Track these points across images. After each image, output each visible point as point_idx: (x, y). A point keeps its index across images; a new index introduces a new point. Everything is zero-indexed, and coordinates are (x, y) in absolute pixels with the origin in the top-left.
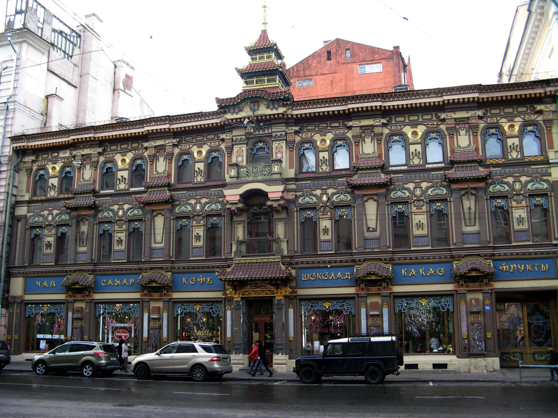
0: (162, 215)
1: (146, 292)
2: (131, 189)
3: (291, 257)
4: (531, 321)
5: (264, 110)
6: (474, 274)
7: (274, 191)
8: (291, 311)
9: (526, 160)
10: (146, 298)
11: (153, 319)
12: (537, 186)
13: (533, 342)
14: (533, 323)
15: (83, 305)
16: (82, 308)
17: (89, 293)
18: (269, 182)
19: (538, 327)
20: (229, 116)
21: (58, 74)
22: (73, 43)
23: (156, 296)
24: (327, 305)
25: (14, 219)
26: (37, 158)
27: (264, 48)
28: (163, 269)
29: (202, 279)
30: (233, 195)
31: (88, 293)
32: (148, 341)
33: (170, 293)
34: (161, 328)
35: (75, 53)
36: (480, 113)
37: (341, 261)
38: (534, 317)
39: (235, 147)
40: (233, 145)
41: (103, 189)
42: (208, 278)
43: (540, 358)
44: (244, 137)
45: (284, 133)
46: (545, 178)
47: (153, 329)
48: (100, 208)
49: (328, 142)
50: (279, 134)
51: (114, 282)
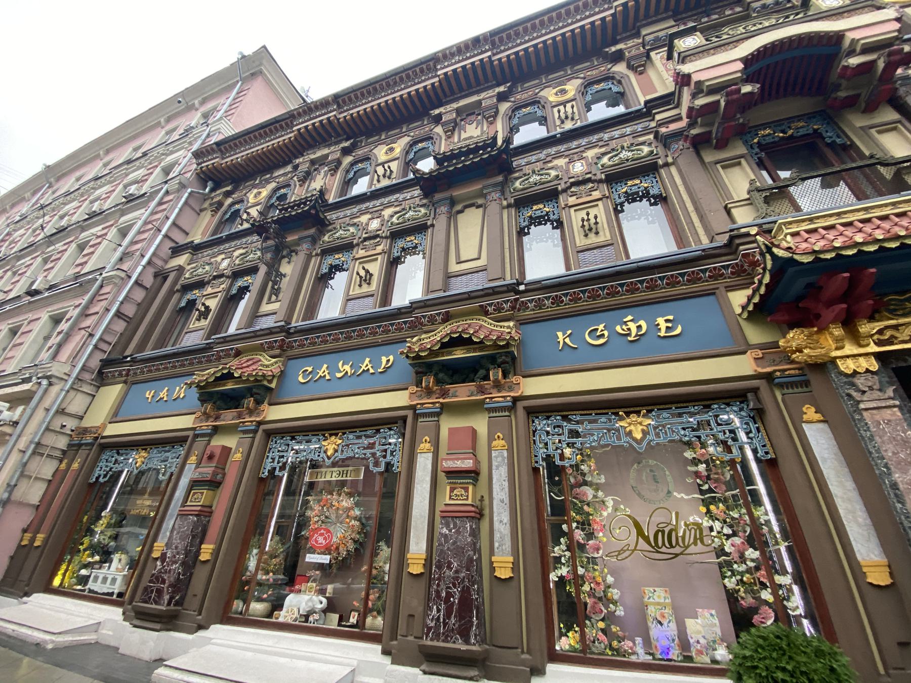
0: (478, 207)
1: (429, 381)
10: (430, 403)
11: (452, 474)
16: (226, 451)
17: (259, 402)
23: (463, 392)
25: (161, 276)
28: (486, 313)
29: (633, 326)
31: (251, 405)
32: (426, 577)
33: (514, 379)
34: (478, 514)
39: (652, 54)
42: (661, 321)
47: (450, 516)
48: (330, 227)
51: (333, 369)
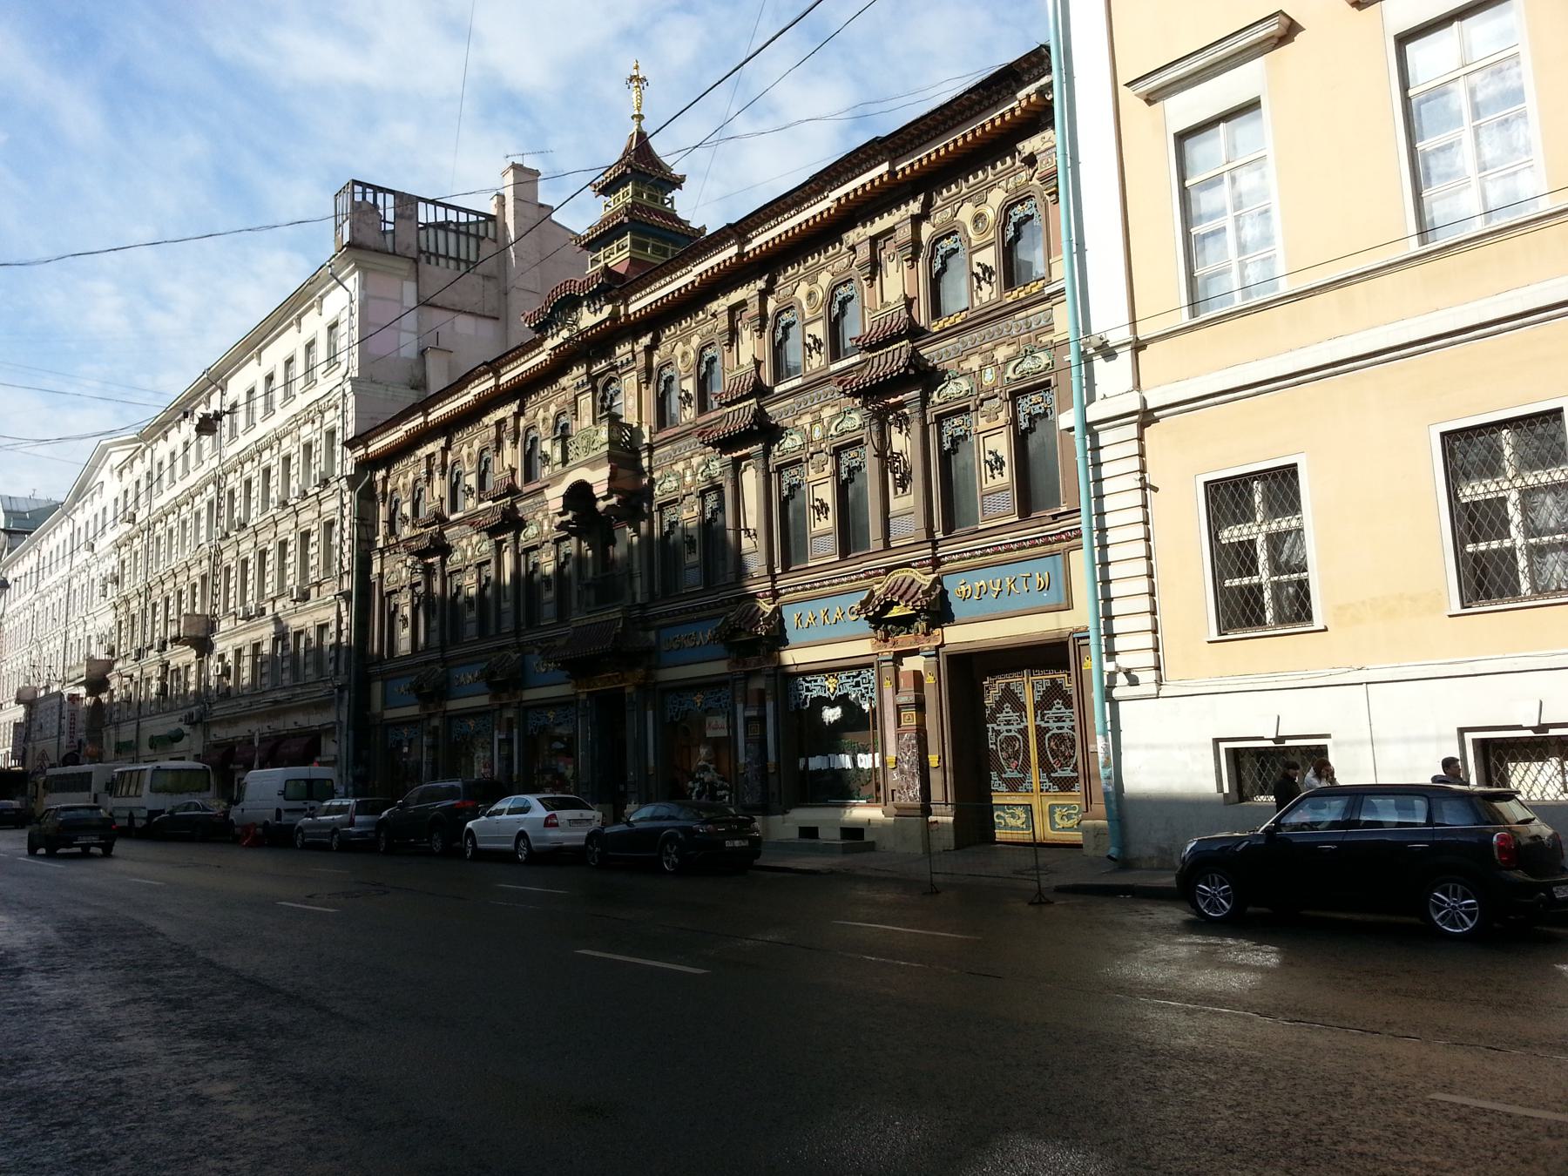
2: (481, 506)
3: (643, 607)
4: (1043, 725)
5: (588, 318)
6: (895, 612)
7: (598, 479)
8: (650, 713)
9: (1009, 300)
12: (1028, 364)
13: (1049, 777)
14: (1048, 730)
15: (436, 722)
16: (436, 728)
18: (592, 464)
19: (1059, 738)
20: (550, 344)
21: (446, 304)
22: (477, 236)
24: (698, 699)
26: (388, 472)
27: (643, 171)
30: (555, 497)
35: (483, 256)
36: (915, 207)
37: (709, 607)
38: (1049, 713)
40: (576, 397)
41: (454, 509)
43: (1068, 823)
44: (585, 378)
45: (630, 356)
46: (1045, 339)
49: (692, 355)
50: (624, 359)
